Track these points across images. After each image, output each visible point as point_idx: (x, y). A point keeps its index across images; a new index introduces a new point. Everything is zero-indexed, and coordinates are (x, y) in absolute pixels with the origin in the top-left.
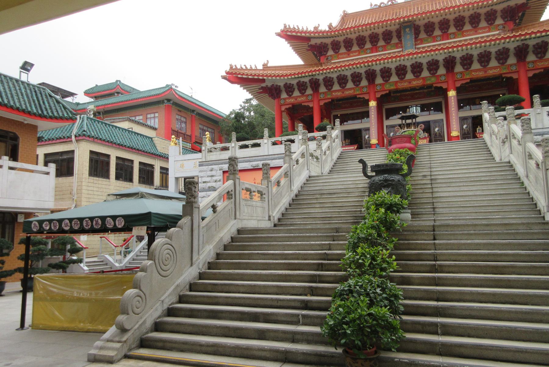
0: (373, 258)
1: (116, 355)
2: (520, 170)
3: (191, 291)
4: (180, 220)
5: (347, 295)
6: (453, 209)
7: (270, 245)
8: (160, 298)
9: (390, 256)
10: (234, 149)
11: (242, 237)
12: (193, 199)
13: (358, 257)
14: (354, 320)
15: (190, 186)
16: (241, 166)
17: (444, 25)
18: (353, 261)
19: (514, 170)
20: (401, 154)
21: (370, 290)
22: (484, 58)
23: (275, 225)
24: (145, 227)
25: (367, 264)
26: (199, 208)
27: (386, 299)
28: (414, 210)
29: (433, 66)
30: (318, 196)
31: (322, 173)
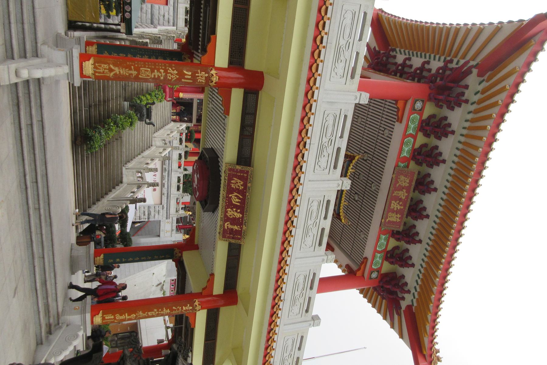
2: (146, 153)
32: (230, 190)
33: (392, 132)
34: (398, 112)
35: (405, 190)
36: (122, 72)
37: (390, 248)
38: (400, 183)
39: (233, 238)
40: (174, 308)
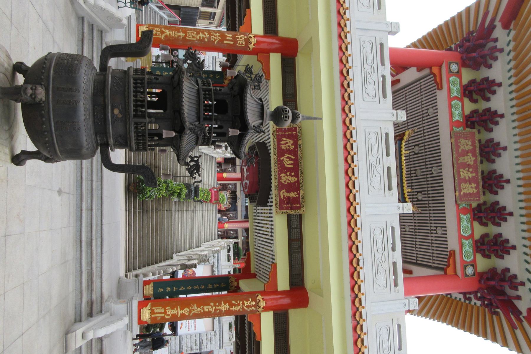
32: (281, 153)
33: (446, 227)
34: (435, 80)
35: (470, 154)
36: (171, 34)
37: (477, 236)
38: (462, 147)
39: (291, 208)
40: (234, 302)
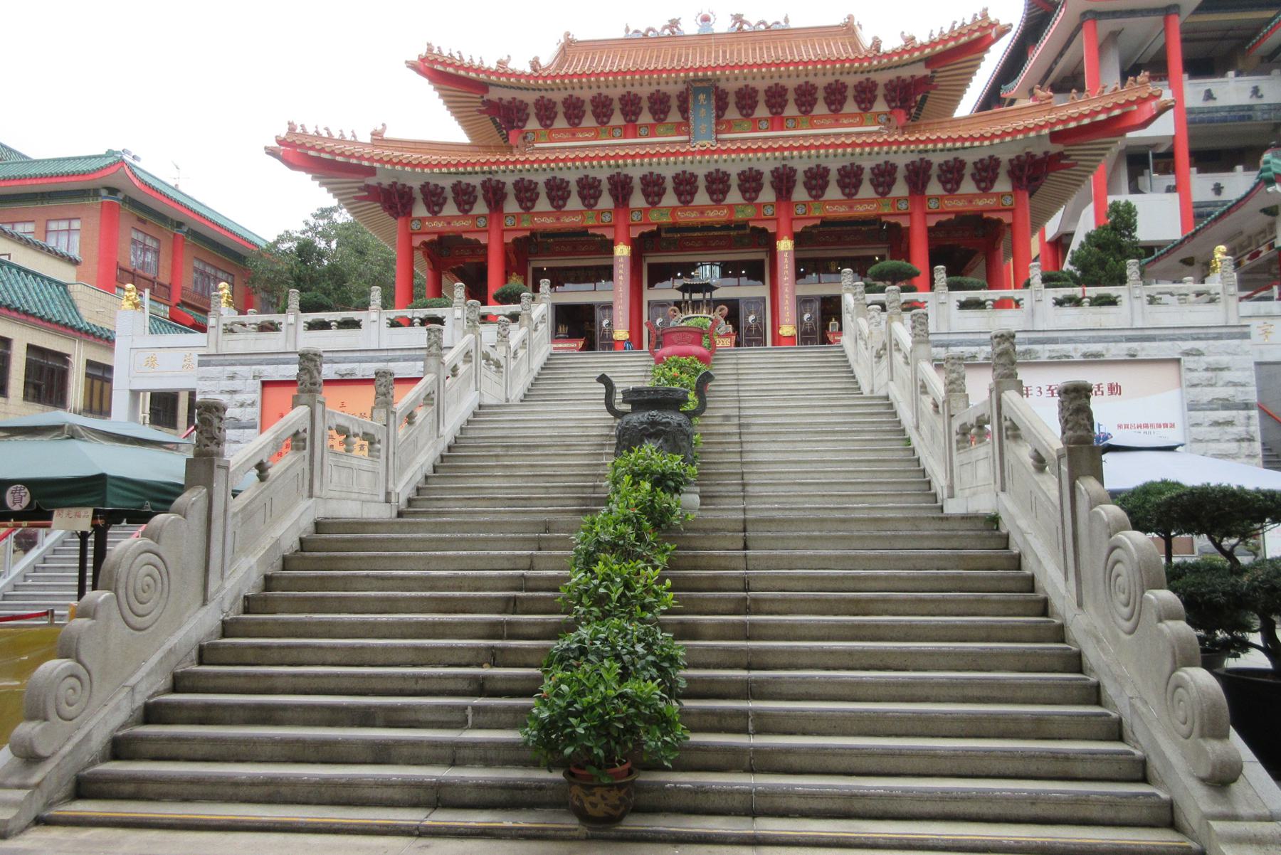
0: (627, 585)
1: (15, 817)
2: (906, 415)
3: (201, 663)
4: (178, 495)
5: (576, 659)
6: (780, 488)
7: (396, 558)
8: (126, 679)
9: (661, 580)
10: (292, 329)
11: (326, 540)
12: (213, 448)
13: (596, 582)
14: (591, 708)
15: (207, 415)
16: (328, 371)
17: (776, 97)
18: (586, 591)
19: (895, 414)
20: (682, 368)
21: (623, 647)
22: (850, 179)
23: (400, 514)
24: (90, 511)
25: (615, 597)
26: (227, 468)
27: (654, 664)
28: (705, 488)
29: (750, 182)
30: (499, 451)
31: (507, 400)
